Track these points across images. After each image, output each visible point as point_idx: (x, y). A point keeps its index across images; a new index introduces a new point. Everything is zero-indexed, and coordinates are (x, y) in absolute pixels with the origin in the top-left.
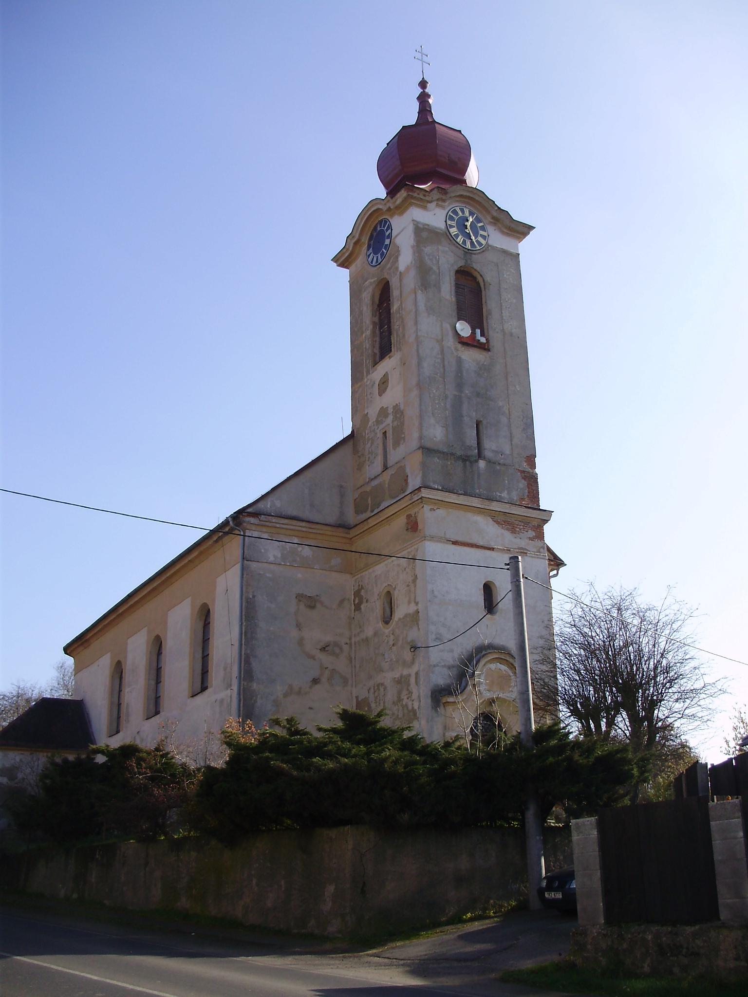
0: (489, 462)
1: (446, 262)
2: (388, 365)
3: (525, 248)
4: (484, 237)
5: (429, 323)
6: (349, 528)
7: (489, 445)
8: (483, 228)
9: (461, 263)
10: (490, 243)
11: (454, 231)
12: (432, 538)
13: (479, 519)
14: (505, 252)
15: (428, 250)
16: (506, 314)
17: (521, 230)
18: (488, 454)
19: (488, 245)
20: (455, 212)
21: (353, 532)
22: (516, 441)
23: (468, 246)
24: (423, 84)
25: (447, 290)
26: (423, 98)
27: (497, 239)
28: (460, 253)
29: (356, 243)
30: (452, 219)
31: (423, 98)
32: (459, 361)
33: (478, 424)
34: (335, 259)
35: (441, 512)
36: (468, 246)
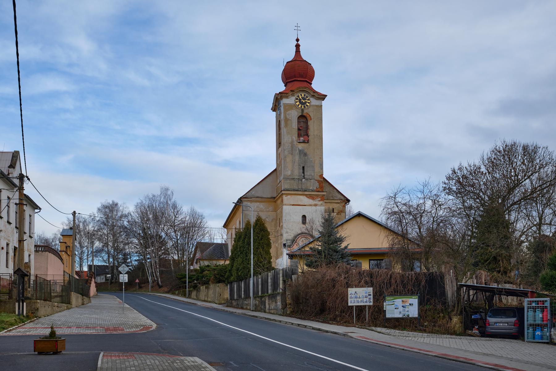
0: (307, 179)
1: (294, 114)
2: (280, 149)
3: (324, 103)
4: (309, 103)
6: (274, 198)
7: (305, 174)
8: (309, 100)
10: (312, 104)
11: (298, 103)
12: (286, 205)
13: (301, 197)
14: (317, 106)
17: (323, 97)
18: (305, 176)
19: (310, 105)
21: (276, 199)
23: (303, 107)
24: (298, 40)
25: (295, 125)
26: (298, 46)
27: (314, 102)
28: (300, 111)
29: (275, 105)
30: (297, 99)
31: (298, 46)
33: (303, 167)
35: (289, 197)
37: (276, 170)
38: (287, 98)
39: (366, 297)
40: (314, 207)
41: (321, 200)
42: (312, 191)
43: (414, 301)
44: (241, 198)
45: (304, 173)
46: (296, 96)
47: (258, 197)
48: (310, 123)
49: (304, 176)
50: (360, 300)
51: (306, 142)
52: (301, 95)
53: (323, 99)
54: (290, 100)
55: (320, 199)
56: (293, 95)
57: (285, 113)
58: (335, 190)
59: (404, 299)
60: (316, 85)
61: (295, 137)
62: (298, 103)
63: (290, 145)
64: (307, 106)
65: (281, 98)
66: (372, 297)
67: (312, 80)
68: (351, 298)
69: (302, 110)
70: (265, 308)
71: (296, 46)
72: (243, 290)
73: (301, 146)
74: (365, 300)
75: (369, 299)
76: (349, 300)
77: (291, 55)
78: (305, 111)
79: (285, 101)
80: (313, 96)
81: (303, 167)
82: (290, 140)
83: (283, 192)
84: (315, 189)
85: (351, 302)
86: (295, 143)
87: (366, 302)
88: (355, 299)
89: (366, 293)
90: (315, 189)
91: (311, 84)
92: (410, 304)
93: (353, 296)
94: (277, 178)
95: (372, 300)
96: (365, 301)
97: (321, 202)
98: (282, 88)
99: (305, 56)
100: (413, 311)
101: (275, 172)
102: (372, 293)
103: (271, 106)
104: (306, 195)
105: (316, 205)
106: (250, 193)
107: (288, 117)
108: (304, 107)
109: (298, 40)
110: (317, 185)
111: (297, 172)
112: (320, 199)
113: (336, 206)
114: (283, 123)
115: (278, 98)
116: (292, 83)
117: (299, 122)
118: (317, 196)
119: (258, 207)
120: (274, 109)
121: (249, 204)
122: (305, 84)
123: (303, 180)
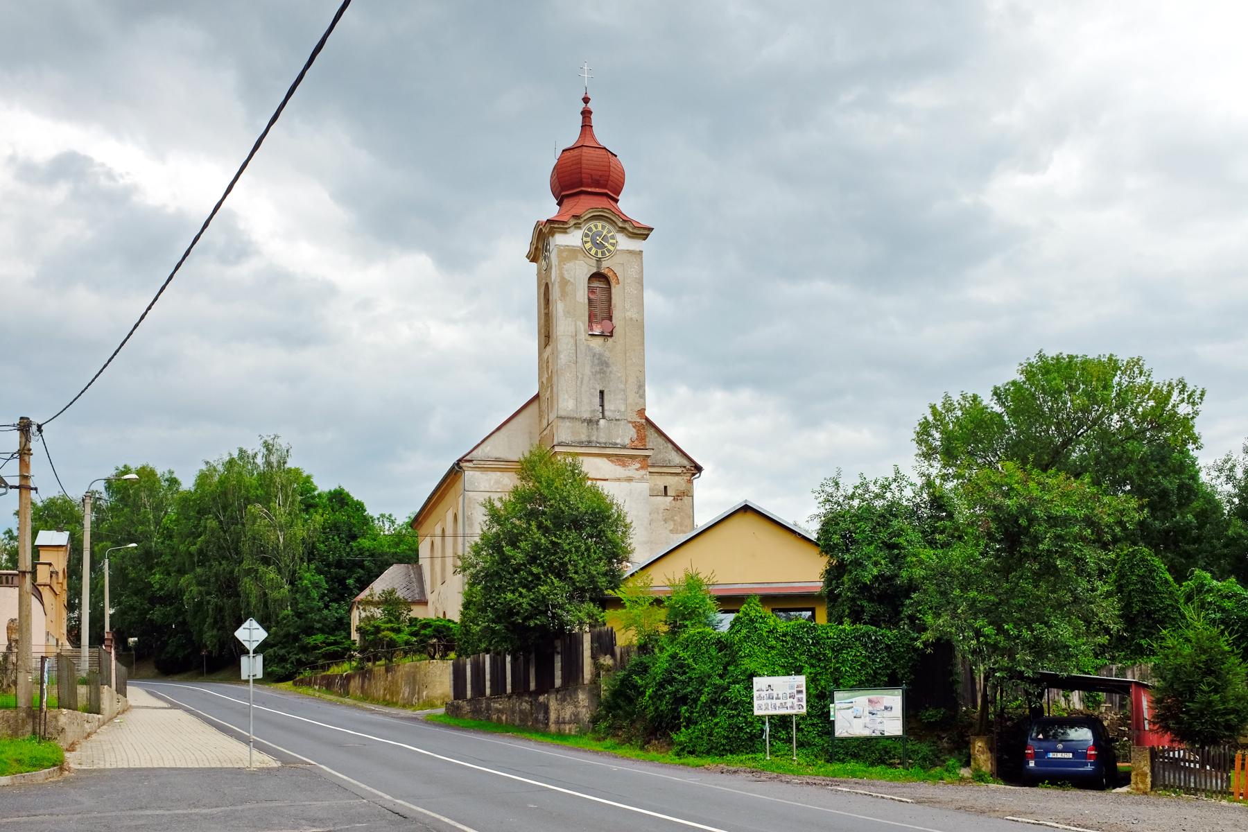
1: (580, 271)
2: (549, 349)
4: (613, 245)
5: (571, 322)
7: (606, 407)
8: (613, 237)
9: (594, 270)
11: (588, 245)
15: (568, 266)
16: (627, 306)
18: (606, 413)
20: (590, 229)
22: (630, 401)
23: (600, 255)
24: (586, 100)
25: (582, 295)
26: (586, 114)
27: (624, 243)
28: (593, 263)
29: (536, 248)
30: (587, 235)
31: (586, 114)
32: (589, 348)
33: (602, 393)
34: (528, 257)
36: (600, 255)
37: (537, 397)
38: (565, 233)
39: (792, 697)
40: (625, 484)
41: (642, 468)
42: (624, 447)
43: (894, 700)
44: (460, 460)
45: (602, 406)
46: (584, 229)
47: (497, 460)
48: (615, 290)
49: (603, 412)
50: (778, 702)
51: (608, 335)
52: (596, 227)
53: (645, 237)
54: (573, 238)
55: (638, 465)
56: (577, 226)
57: (561, 269)
58: (670, 446)
59: (871, 697)
60: (628, 204)
61: (582, 325)
62: (588, 245)
63: (572, 341)
64: (609, 251)
65: (552, 232)
66: (804, 696)
67: (618, 193)
68: (760, 698)
69: (599, 260)
70: (548, 719)
71: (583, 113)
72: (488, 677)
73: (597, 343)
74: (789, 702)
75: (799, 700)
76: (756, 703)
77: (571, 136)
78: (605, 264)
79: (559, 240)
80: (622, 230)
81: (602, 393)
82: (572, 329)
83: (557, 449)
84: (627, 441)
85: (760, 708)
86: (583, 335)
87: (792, 707)
88: (769, 701)
89: (792, 687)
90: (627, 441)
91: (617, 201)
92: (886, 708)
93: (763, 694)
94: (541, 417)
95: (804, 704)
96: (789, 705)
97: (642, 472)
98: (550, 208)
99: (603, 134)
100: (893, 726)
101: (535, 406)
102: (804, 689)
103: (526, 248)
104: (608, 456)
105: (630, 479)
106: (480, 449)
107: (567, 276)
108: (603, 253)
109: (586, 100)
110: (632, 433)
111: (589, 407)
112: (638, 465)
113: (671, 481)
114: (555, 292)
115: (543, 234)
116: (576, 199)
117: (591, 290)
118: (632, 457)
119: (497, 482)
120: (534, 257)
121: (478, 474)
122: (604, 202)
123: (602, 422)
